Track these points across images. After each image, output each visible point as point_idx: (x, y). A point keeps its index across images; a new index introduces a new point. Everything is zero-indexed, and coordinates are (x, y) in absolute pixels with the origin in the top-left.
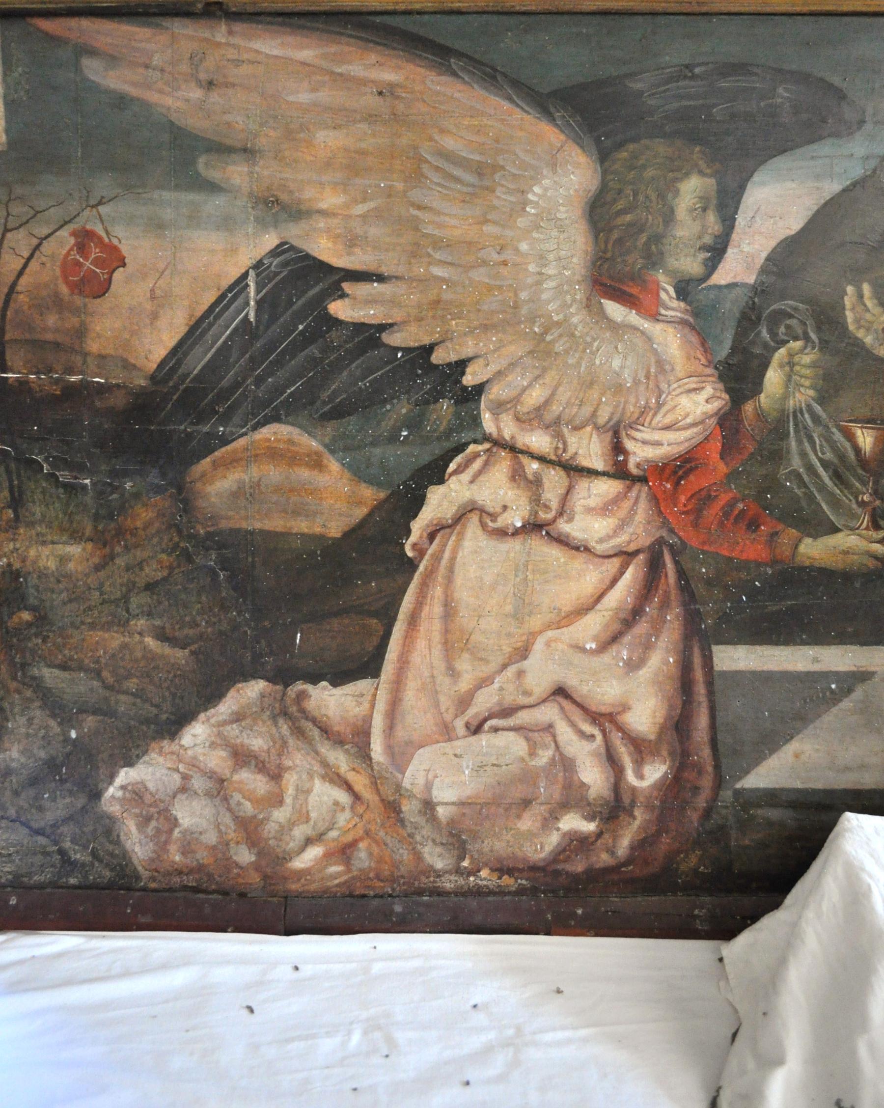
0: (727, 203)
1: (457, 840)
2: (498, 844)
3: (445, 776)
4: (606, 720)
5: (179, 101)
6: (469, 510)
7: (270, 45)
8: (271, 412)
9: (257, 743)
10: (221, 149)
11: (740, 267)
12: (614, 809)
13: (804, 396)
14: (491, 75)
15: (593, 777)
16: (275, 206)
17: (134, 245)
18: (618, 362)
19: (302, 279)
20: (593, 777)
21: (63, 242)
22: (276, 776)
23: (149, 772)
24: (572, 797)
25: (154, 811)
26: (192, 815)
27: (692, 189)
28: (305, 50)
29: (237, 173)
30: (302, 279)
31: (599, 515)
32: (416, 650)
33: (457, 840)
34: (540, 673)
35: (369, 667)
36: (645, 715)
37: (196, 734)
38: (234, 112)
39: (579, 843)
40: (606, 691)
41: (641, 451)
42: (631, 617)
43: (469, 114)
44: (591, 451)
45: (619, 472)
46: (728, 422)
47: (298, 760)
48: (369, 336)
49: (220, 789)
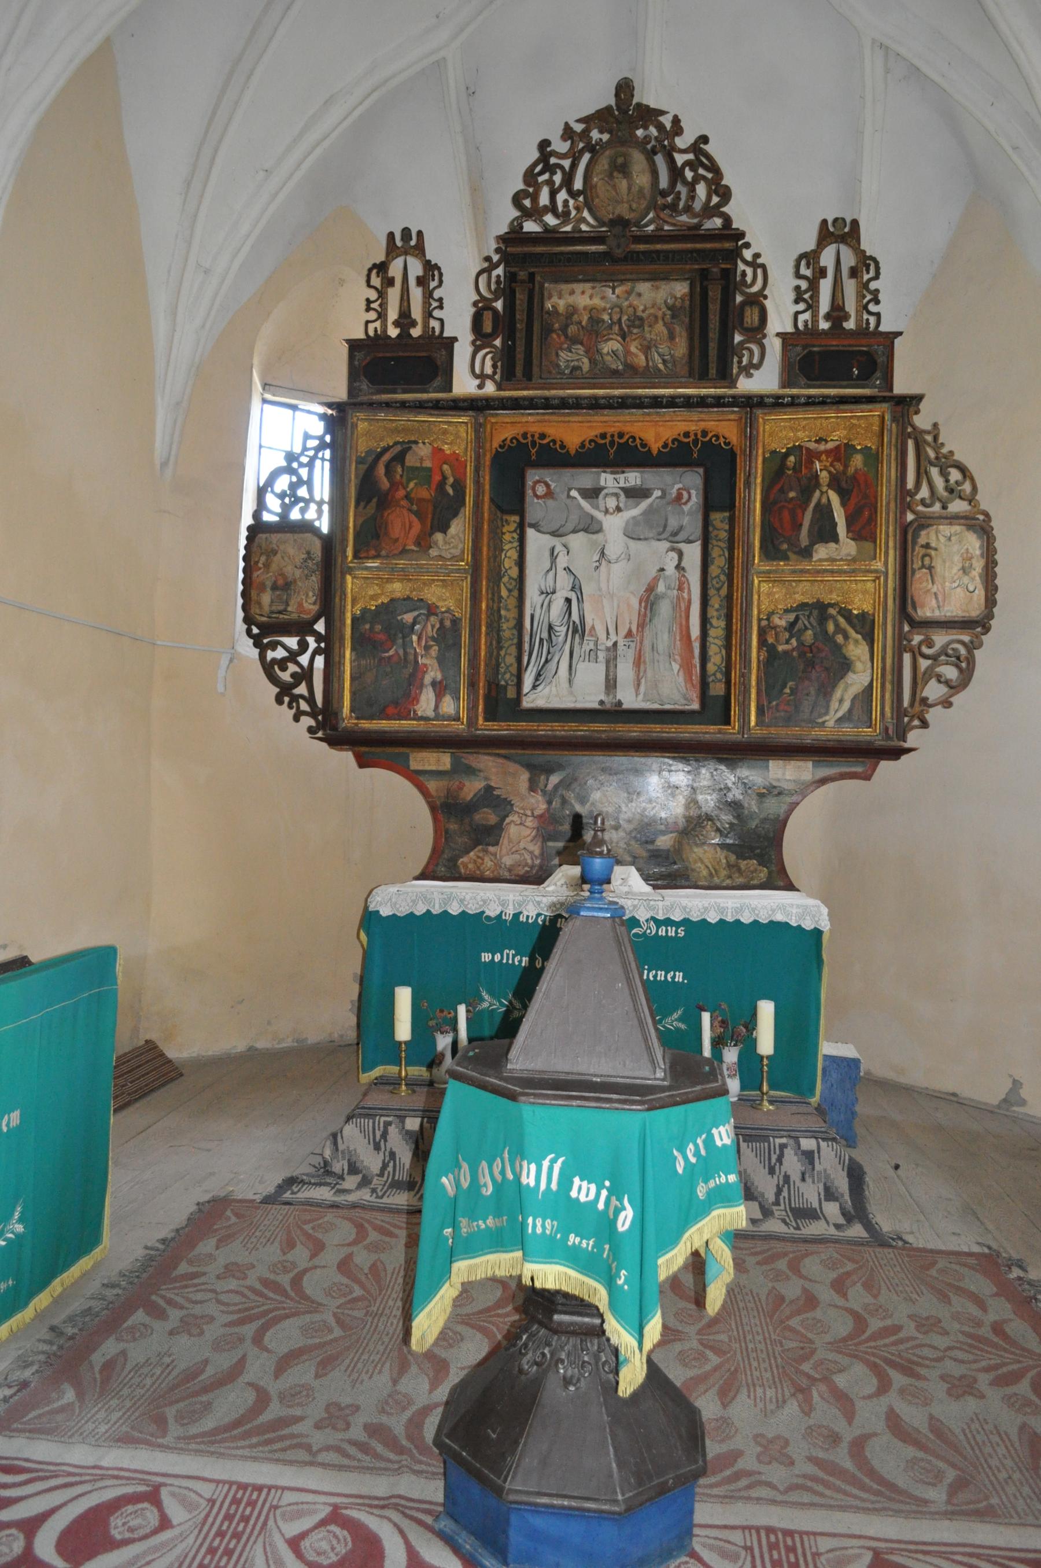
0: (548, 780)
1: (510, 870)
2: (516, 872)
3: (508, 861)
4: (531, 853)
5: (474, 765)
6: (512, 821)
7: (486, 757)
8: (487, 807)
9: (481, 855)
10: (480, 771)
11: (550, 787)
12: (532, 867)
13: (558, 806)
14: (515, 762)
15: (529, 861)
16: (486, 779)
17: (467, 784)
18: (533, 801)
19: (489, 789)
20: (529, 861)
21: (457, 783)
22: (483, 860)
23: (465, 859)
24: (526, 865)
25: (465, 866)
26: (470, 866)
27: (543, 777)
28: (491, 758)
29: (482, 774)
30: (489, 789)
31: (530, 822)
32: (504, 841)
33: (510, 870)
34: (522, 845)
35: (497, 844)
36: (537, 852)
37: (472, 854)
38: (481, 766)
39: (527, 872)
40: (531, 847)
41: (536, 814)
42: (535, 837)
43: (512, 767)
44: (529, 813)
45: (533, 815)
46: (548, 810)
47: (487, 859)
48: (498, 796)
49: (475, 862)
